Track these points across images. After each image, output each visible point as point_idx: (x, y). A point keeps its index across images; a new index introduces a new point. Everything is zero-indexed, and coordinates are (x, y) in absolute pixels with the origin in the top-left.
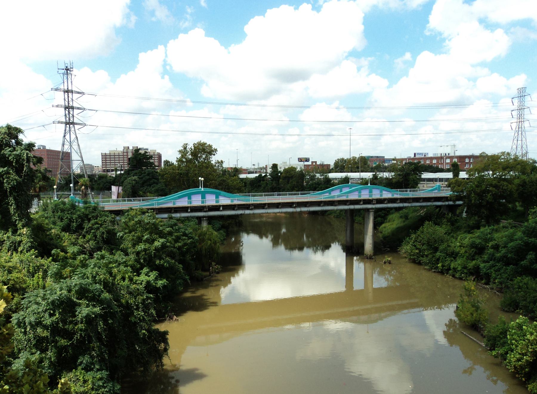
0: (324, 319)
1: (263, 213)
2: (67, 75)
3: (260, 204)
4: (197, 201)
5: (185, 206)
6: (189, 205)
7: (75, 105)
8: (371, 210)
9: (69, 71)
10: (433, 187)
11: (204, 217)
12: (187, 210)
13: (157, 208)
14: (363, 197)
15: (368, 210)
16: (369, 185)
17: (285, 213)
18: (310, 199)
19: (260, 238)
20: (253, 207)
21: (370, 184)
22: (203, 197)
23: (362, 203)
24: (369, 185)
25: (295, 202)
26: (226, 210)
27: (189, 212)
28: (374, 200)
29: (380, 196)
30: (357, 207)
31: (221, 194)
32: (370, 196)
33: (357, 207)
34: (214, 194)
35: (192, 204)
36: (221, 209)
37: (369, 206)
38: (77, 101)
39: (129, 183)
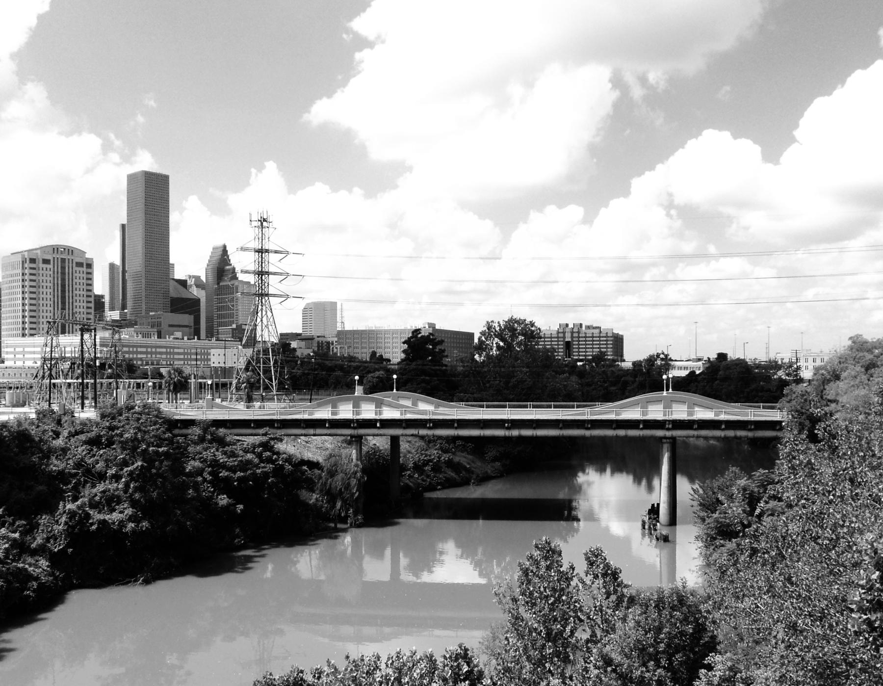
0: (365, 641)
1: (688, 437)
2: (262, 228)
3: (443, 419)
4: (656, 413)
5: (630, 419)
6: (377, 417)
7: (272, 269)
8: (665, 441)
9: (265, 224)
10: (321, 399)
11: (665, 438)
12: (300, 424)
13: (279, 420)
14: (651, 416)
15: (660, 439)
16: (395, 391)
17: (717, 439)
18: (537, 416)
19: (690, 482)
20: (431, 425)
21: (397, 390)
22: (356, 405)
23: (696, 426)
24: (395, 391)
25: (508, 420)
26: (241, 428)
27: (642, 429)
28: (667, 422)
29: (664, 416)
30: (488, 432)
31: (384, 403)
32: (690, 413)
33: (488, 432)
34: (373, 402)
35: (384, 416)
36: (456, 425)
37: (660, 433)
38: (273, 262)
39: (370, 381)
